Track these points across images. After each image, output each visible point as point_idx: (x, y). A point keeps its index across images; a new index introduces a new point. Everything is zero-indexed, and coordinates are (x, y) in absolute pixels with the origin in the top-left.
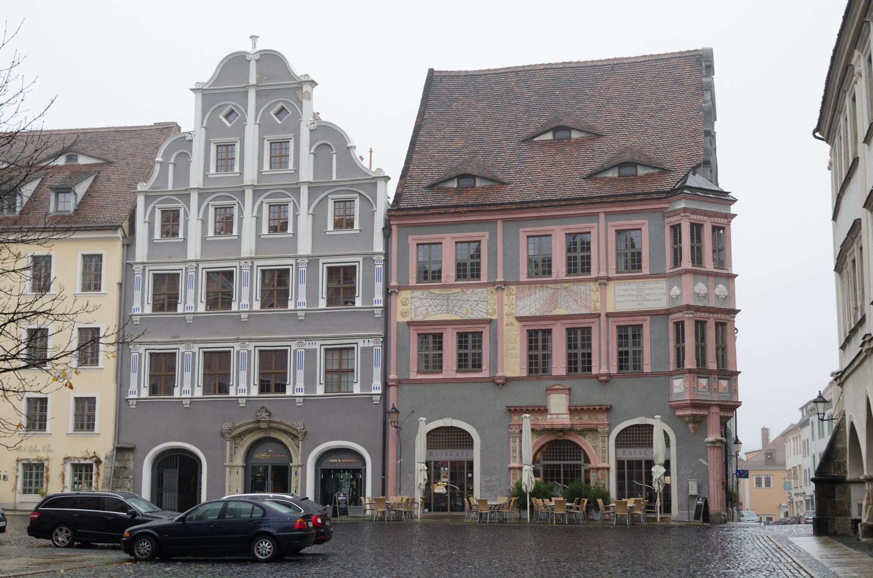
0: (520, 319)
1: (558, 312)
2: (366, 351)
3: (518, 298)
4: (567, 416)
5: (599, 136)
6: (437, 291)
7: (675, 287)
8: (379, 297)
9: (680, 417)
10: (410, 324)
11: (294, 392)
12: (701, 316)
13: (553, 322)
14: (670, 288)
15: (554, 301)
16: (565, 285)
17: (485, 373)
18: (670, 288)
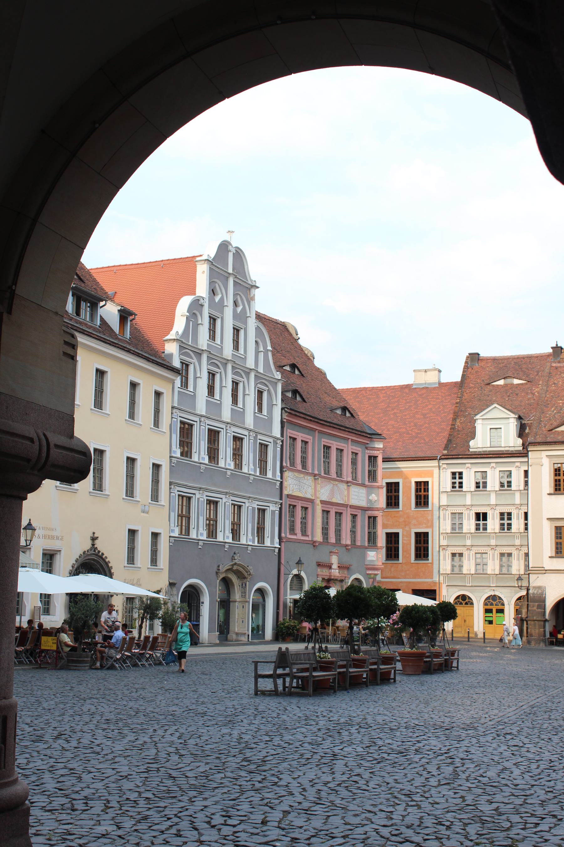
0: (322, 502)
1: (334, 500)
2: (273, 512)
3: (321, 487)
4: (337, 571)
5: (302, 375)
6: (296, 474)
7: (373, 495)
8: (278, 473)
9: (368, 574)
10: (288, 496)
11: (197, 536)
12: (340, 509)
13: (331, 507)
14: (368, 494)
15: (332, 493)
16: (337, 483)
17: (310, 538)
18: (368, 494)
